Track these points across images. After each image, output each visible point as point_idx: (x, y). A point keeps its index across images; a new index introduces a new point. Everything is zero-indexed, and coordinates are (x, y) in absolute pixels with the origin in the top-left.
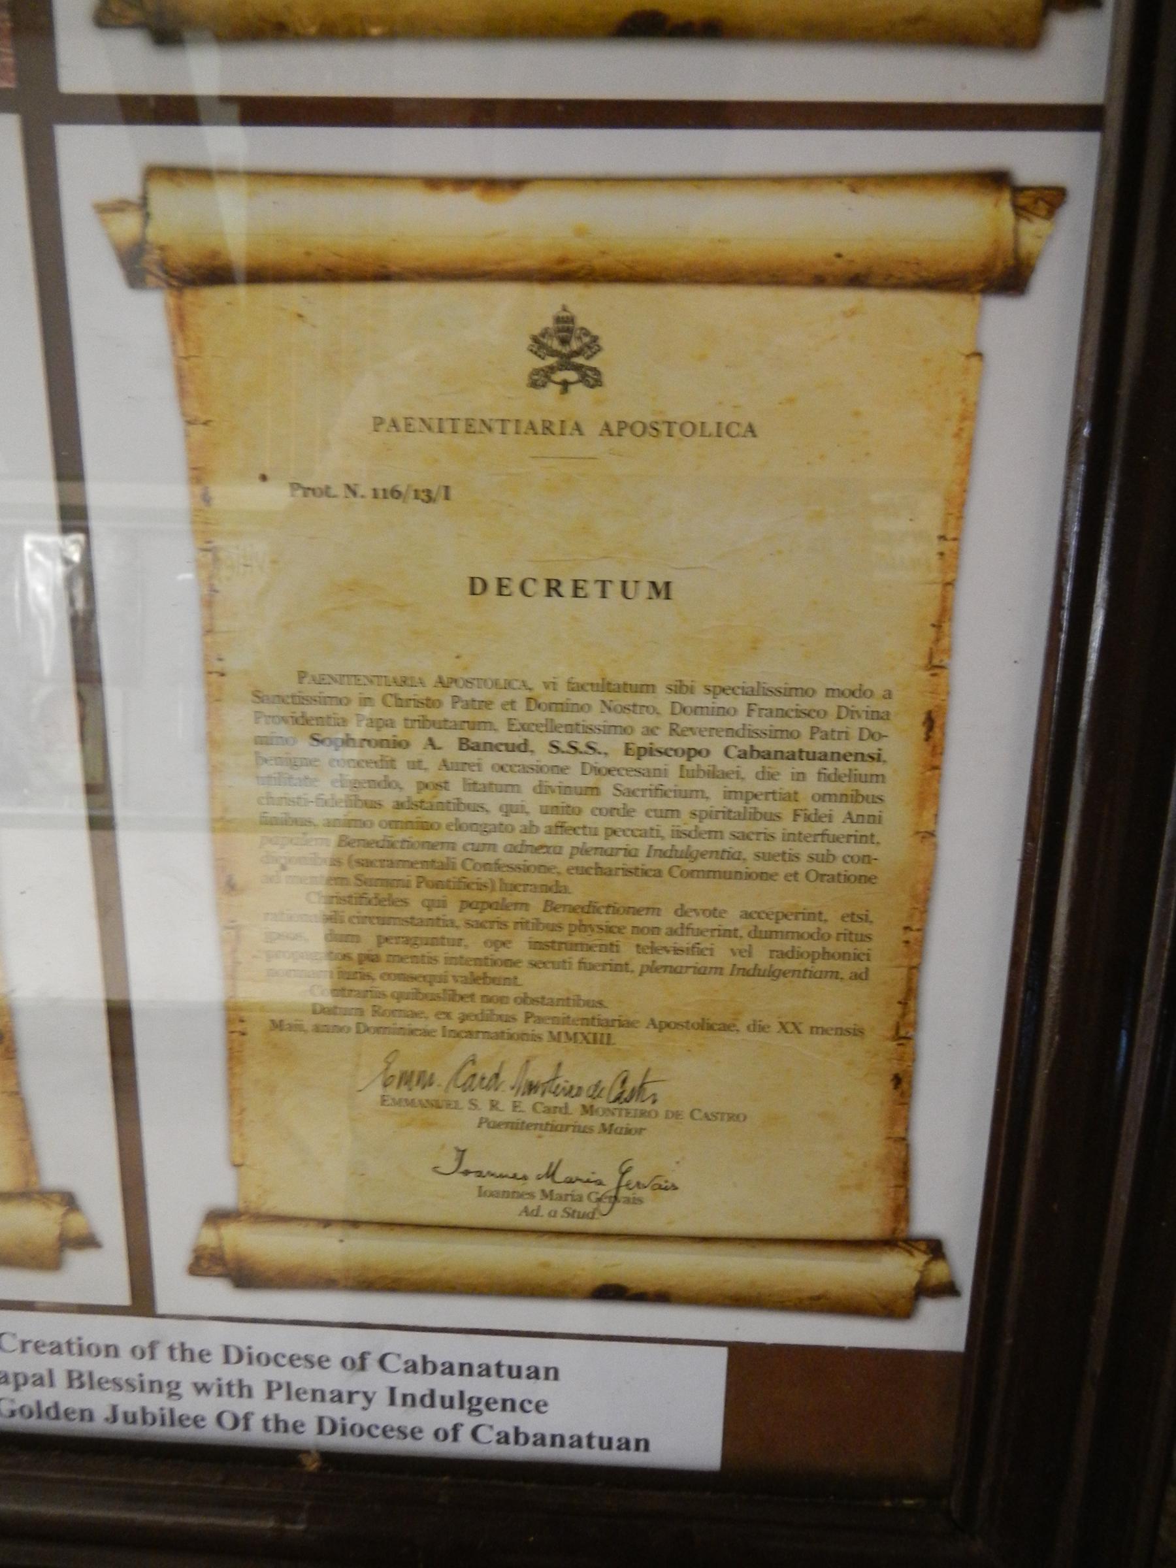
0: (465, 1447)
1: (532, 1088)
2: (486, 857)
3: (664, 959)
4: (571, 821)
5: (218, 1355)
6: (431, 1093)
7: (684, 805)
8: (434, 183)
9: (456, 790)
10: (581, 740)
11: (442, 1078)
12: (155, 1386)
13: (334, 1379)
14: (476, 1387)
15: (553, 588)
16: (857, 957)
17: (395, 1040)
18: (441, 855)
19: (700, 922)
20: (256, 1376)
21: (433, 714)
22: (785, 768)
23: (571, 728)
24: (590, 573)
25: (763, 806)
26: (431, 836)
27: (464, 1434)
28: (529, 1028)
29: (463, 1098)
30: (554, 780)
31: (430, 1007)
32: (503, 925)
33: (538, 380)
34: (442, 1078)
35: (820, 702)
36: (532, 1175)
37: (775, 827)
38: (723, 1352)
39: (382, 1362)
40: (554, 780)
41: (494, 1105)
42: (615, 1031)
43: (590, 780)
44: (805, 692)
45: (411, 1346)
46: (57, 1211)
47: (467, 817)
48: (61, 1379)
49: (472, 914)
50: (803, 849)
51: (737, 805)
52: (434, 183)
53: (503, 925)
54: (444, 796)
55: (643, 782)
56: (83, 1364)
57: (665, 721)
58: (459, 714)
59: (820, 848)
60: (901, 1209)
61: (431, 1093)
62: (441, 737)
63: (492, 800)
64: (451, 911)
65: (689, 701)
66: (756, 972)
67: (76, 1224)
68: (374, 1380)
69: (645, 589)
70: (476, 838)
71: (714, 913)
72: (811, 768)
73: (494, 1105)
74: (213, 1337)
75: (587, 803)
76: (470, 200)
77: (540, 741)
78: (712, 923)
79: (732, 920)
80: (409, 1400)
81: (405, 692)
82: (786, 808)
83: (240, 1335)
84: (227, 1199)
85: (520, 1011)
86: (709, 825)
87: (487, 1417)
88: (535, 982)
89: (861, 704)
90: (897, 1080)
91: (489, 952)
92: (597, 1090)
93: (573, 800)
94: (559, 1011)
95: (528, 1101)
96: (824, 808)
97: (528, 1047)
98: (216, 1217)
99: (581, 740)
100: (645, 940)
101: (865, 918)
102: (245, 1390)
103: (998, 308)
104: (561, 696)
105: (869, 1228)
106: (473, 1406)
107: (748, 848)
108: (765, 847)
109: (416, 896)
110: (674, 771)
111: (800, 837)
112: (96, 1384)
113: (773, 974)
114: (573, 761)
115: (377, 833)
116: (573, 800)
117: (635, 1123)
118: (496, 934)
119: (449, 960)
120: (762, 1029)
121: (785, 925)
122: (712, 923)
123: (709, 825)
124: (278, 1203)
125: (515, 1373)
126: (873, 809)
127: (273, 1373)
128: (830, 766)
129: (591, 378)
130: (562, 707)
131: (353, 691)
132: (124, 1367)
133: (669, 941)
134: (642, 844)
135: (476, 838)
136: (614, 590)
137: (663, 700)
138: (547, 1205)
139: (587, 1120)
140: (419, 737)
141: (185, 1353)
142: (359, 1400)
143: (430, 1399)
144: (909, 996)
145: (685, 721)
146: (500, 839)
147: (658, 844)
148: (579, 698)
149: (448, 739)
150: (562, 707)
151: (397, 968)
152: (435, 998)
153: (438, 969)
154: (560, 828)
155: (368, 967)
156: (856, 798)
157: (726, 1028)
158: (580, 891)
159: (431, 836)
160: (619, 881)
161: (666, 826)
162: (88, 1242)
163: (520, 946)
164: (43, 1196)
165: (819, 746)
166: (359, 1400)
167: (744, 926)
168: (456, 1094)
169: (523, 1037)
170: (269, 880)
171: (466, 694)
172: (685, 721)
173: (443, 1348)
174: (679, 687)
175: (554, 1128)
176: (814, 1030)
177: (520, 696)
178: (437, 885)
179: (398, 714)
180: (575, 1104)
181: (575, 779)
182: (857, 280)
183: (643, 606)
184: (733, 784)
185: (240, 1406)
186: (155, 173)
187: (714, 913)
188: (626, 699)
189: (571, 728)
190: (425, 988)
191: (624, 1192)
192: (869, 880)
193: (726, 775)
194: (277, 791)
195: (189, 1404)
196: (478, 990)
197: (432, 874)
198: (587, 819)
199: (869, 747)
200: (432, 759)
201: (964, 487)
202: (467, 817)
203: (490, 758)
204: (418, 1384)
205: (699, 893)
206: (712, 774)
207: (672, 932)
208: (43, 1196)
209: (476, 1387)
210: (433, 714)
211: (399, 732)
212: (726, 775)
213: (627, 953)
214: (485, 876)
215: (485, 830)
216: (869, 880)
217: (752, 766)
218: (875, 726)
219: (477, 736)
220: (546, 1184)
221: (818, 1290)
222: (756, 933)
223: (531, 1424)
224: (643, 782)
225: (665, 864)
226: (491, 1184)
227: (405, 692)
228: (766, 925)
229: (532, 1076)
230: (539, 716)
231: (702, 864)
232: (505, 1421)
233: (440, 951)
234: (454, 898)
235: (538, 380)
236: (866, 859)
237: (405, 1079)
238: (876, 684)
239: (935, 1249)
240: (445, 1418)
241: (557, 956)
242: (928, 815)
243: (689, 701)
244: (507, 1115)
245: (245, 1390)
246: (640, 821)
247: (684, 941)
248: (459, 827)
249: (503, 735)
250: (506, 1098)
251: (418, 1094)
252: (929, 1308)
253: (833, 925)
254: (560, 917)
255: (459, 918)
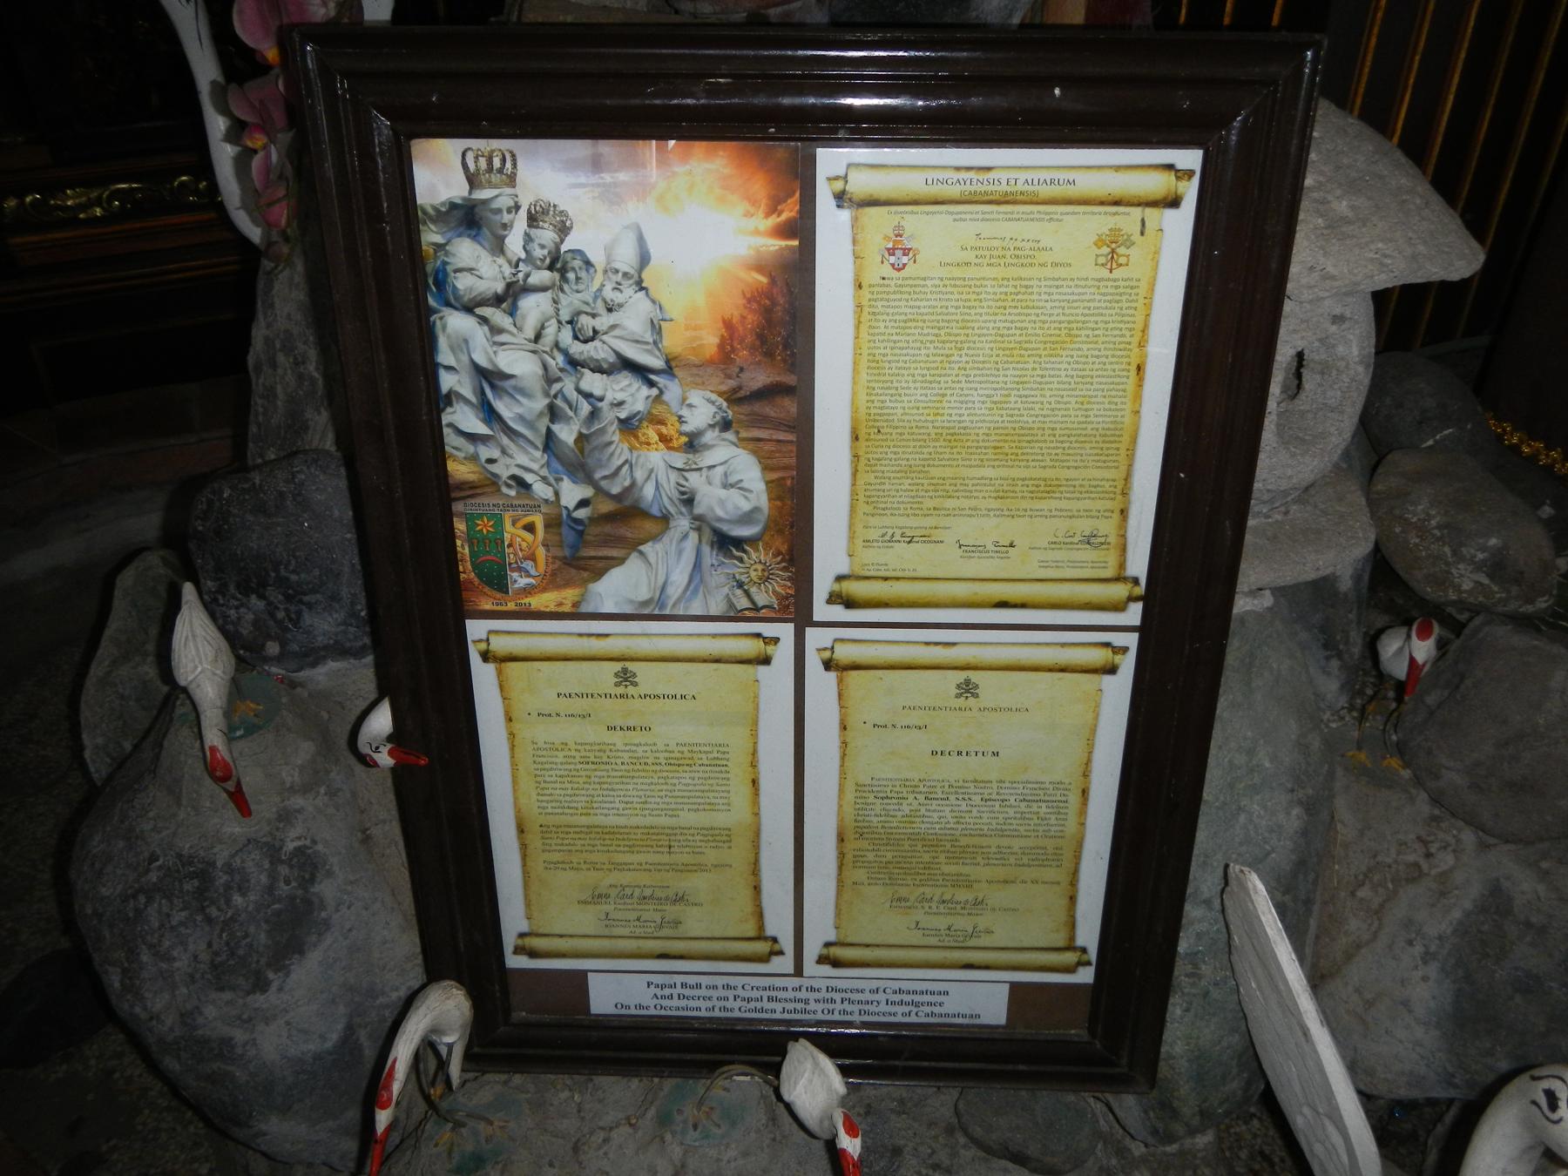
0: (913, 1019)
1: (944, 902)
2: (933, 831)
3: (991, 862)
4: (963, 821)
5: (824, 989)
6: (908, 904)
7: (1001, 816)
8: (927, 644)
9: (923, 811)
10: (966, 797)
11: (912, 899)
12: (800, 1001)
13: (867, 996)
14: (917, 998)
15: (959, 753)
16: (1058, 860)
17: (896, 887)
18: (916, 831)
19: (1004, 850)
20: (837, 997)
21: (916, 790)
22: (1035, 805)
23: (963, 793)
24: (972, 749)
25: (1027, 816)
26: (914, 825)
27: (913, 1014)
28: (945, 883)
29: (919, 906)
30: (956, 809)
31: (909, 878)
32: (936, 852)
33: (958, 696)
34: (912, 899)
35: (1047, 786)
36: (942, 928)
37: (1032, 822)
38: (1008, 985)
39: (884, 991)
40: (956, 809)
41: (930, 907)
42: (975, 885)
43: (969, 808)
44: (1042, 783)
45: (896, 985)
46: (770, 943)
47: (926, 820)
48: (765, 999)
49: (927, 849)
50: (1041, 829)
51: (1019, 816)
52: (927, 644)
53: (936, 852)
54: (918, 814)
55: (987, 809)
56: (773, 994)
57: (995, 791)
58: (925, 789)
59: (1046, 828)
60: (1072, 938)
61: (908, 904)
62: (918, 796)
63: (935, 815)
64: (919, 848)
65: (1004, 785)
66: (1023, 865)
67: (776, 947)
68: (881, 997)
69: (990, 753)
70: (929, 826)
71: (1009, 848)
72: (1044, 805)
73: (930, 907)
74: (822, 984)
75: (967, 815)
76: (939, 649)
77: (952, 798)
78: (1009, 851)
79: (1016, 849)
80: (893, 1003)
81: (907, 783)
82: (1035, 817)
83: (833, 983)
84: (832, 938)
85: (940, 878)
86: (1009, 821)
87: (922, 1008)
88: (947, 869)
89: (1062, 786)
90: (1071, 898)
91: (931, 860)
92: (967, 901)
93: (963, 815)
94: (955, 878)
95: (942, 906)
96: (1048, 816)
97: (943, 889)
98: (828, 945)
99: (966, 797)
100: (985, 856)
101: (1061, 849)
102: (833, 1001)
103: (1107, 679)
104: (961, 784)
105: (1061, 944)
106: (917, 1005)
107: (1022, 828)
108: (1027, 828)
109: (907, 843)
110: (997, 806)
111: (1039, 825)
112: (777, 1000)
113: (1029, 866)
114: (964, 803)
115: (895, 825)
116: (963, 815)
117: (979, 912)
118: (934, 854)
119: (917, 863)
120: (1025, 882)
121: (1033, 851)
122: (1009, 851)
123: (1009, 821)
124: (850, 940)
125: (932, 993)
126: (1064, 816)
127: (844, 995)
128: (1050, 804)
129: (976, 696)
130: (960, 787)
131: (890, 783)
132: (790, 994)
133: (994, 856)
134: (986, 827)
135: (929, 826)
136: (980, 755)
137: (995, 785)
138: (947, 939)
139: (962, 912)
140: (911, 797)
141: (812, 989)
142: (875, 1003)
143: (901, 1003)
144: (1075, 872)
145: (1002, 791)
146: (937, 826)
147: (991, 827)
148: (966, 785)
149: (921, 798)
150: (960, 787)
151: (897, 866)
152: (911, 874)
153: (914, 865)
154: (958, 823)
155: (889, 865)
156: (1059, 813)
157: (1013, 882)
158: (964, 841)
159: (914, 825)
160: (976, 838)
161: (994, 822)
162: (781, 953)
163: (942, 858)
164: (765, 939)
165: (1047, 798)
166: (875, 1003)
167: (1020, 851)
168: (916, 904)
169: (942, 886)
170: (855, 839)
171: (928, 784)
172: (1002, 791)
173: (905, 986)
174: (1001, 781)
175: (951, 914)
176: (1043, 882)
177: (947, 784)
178: (914, 840)
179: (904, 790)
180: (959, 907)
181: (964, 808)
182: (1063, 670)
183: (989, 759)
184: (1017, 809)
185: (831, 1006)
186: (836, 640)
187: (1009, 848)
188: (982, 785)
189: (963, 793)
190: (907, 871)
191: (975, 934)
192: (1062, 837)
193: (1015, 807)
194: (861, 813)
195: (812, 1006)
196: (927, 872)
197: (913, 837)
198: (968, 820)
199: (1063, 799)
200: (915, 803)
201: (1096, 726)
202: (926, 820)
203: (935, 802)
204: (897, 998)
205: (1005, 842)
206: (1011, 806)
207: (995, 853)
208: (765, 939)
209: (917, 998)
210: (916, 790)
211: (905, 795)
212: (1015, 807)
213: (979, 859)
214: (931, 837)
215: (932, 823)
216: (1062, 837)
217: (1023, 805)
218: (1065, 792)
219: (930, 796)
220: (948, 932)
221: (1042, 964)
222: (1024, 853)
223: (937, 1010)
224: (987, 809)
225: (993, 833)
226: (926, 932)
227: (907, 783)
228: (1026, 851)
229: (945, 898)
230: (953, 790)
231: (1008, 833)
232: (928, 1009)
233: (914, 860)
234: (920, 844)
235: (958, 696)
236: (1062, 831)
237: (899, 900)
238: (1067, 781)
239: (1084, 950)
240: (906, 1009)
241: (955, 861)
242: (1083, 817)
243: (1004, 785)
244: (935, 910)
245: (833, 1001)
246: (985, 820)
247: (998, 856)
248: (923, 822)
249: (940, 796)
250: (934, 905)
251: (903, 904)
252: (1081, 970)
253: (1050, 851)
254: (958, 849)
255: (921, 850)
